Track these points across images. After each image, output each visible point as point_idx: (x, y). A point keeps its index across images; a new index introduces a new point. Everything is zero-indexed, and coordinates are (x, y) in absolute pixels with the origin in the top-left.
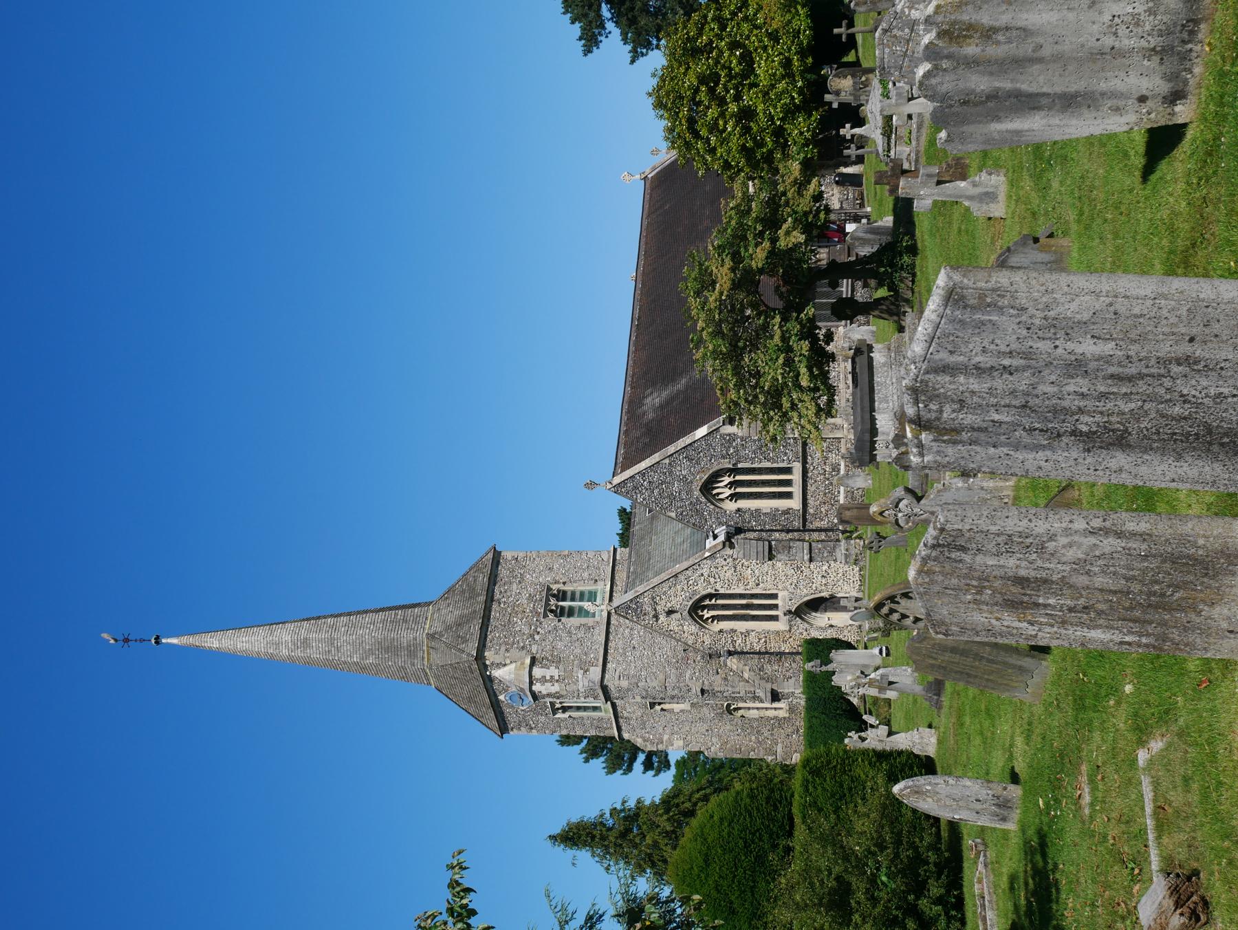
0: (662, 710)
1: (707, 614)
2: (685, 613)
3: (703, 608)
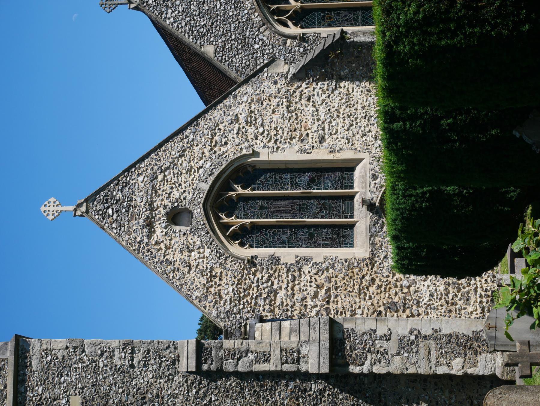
2: (198, 211)
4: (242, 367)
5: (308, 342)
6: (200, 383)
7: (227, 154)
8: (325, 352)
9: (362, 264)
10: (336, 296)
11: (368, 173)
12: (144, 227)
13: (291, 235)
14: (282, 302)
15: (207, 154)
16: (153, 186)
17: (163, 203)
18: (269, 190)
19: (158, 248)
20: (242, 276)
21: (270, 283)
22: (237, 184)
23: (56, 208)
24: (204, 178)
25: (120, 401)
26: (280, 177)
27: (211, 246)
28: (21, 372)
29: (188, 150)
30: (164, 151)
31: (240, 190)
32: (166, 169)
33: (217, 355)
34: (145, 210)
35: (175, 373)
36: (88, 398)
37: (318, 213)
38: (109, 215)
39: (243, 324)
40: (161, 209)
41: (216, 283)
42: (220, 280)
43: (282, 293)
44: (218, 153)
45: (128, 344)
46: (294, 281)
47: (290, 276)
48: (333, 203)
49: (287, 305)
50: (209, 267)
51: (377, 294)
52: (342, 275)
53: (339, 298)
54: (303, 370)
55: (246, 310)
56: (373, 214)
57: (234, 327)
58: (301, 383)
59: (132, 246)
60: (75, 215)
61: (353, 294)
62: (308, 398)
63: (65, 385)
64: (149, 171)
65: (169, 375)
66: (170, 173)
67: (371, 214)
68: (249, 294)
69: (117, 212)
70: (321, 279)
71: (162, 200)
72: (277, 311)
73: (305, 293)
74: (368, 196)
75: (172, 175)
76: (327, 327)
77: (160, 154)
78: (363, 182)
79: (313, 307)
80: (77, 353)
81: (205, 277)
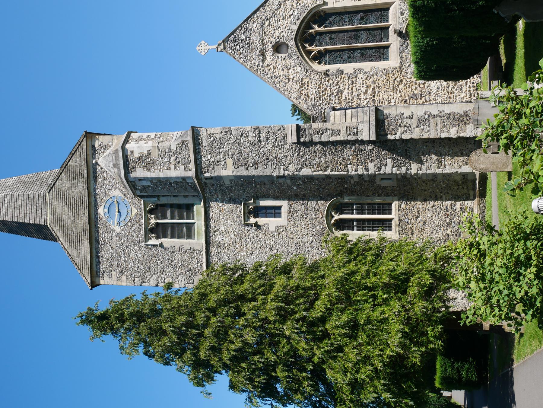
0: (257, 226)
1: (315, 49)
2: (292, 44)
3: (311, 39)
4: (324, 139)
5: (362, 122)
6: (300, 149)
7: (307, 5)
8: (373, 128)
9: (395, 71)
10: (379, 92)
11: (398, 11)
12: (259, 56)
13: (350, 55)
14: (346, 98)
15: (295, 6)
16: (263, 30)
17: (270, 40)
18: (335, 26)
19: (269, 68)
20: (321, 83)
21: (338, 86)
22: (315, 24)
23: (206, 48)
24: (294, 22)
25: (255, 161)
26: (342, 18)
27: (301, 66)
28: (197, 147)
29: (283, 4)
30: (268, 6)
31: (317, 28)
32: (270, 18)
33: (309, 132)
34: (259, 45)
35: (285, 144)
36: (236, 160)
37: (366, 40)
38: (238, 50)
39: (323, 112)
40: (269, 44)
41: (305, 88)
42: (308, 86)
43: (345, 92)
44: (302, 5)
45: (256, 128)
46: (352, 84)
47: (350, 81)
48: (376, 32)
49: (349, 99)
50: (300, 78)
51: (404, 89)
52: (382, 79)
53: (381, 93)
54: (360, 139)
55: (324, 104)
56: (401, 38)
57: (317, 114)
58: (359, 146)
59: (253, 68)
60: (217, 51)
61: (389, 90)
62: (363, 154)
63: (223, 153)
64: (259, 20)
65: (281, 145)
66: (273, 20)
67: (400, 38)
68: (325, 93)
69: (242, 47)
70: (369, 82)
71: (269, 38)
72: (343, 103)
73: (360, 91)
74: (398, 27)
75: (274, 21)
76: (374, 113)
77: (265, 8)
78: (395, 18)
79: (365, 100)
80: (228, 135)
81: (298, 85)
